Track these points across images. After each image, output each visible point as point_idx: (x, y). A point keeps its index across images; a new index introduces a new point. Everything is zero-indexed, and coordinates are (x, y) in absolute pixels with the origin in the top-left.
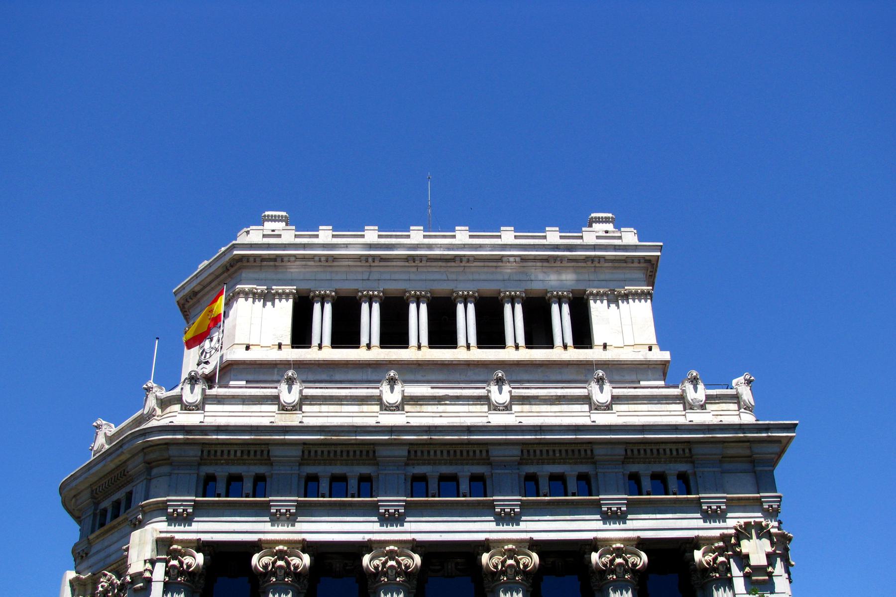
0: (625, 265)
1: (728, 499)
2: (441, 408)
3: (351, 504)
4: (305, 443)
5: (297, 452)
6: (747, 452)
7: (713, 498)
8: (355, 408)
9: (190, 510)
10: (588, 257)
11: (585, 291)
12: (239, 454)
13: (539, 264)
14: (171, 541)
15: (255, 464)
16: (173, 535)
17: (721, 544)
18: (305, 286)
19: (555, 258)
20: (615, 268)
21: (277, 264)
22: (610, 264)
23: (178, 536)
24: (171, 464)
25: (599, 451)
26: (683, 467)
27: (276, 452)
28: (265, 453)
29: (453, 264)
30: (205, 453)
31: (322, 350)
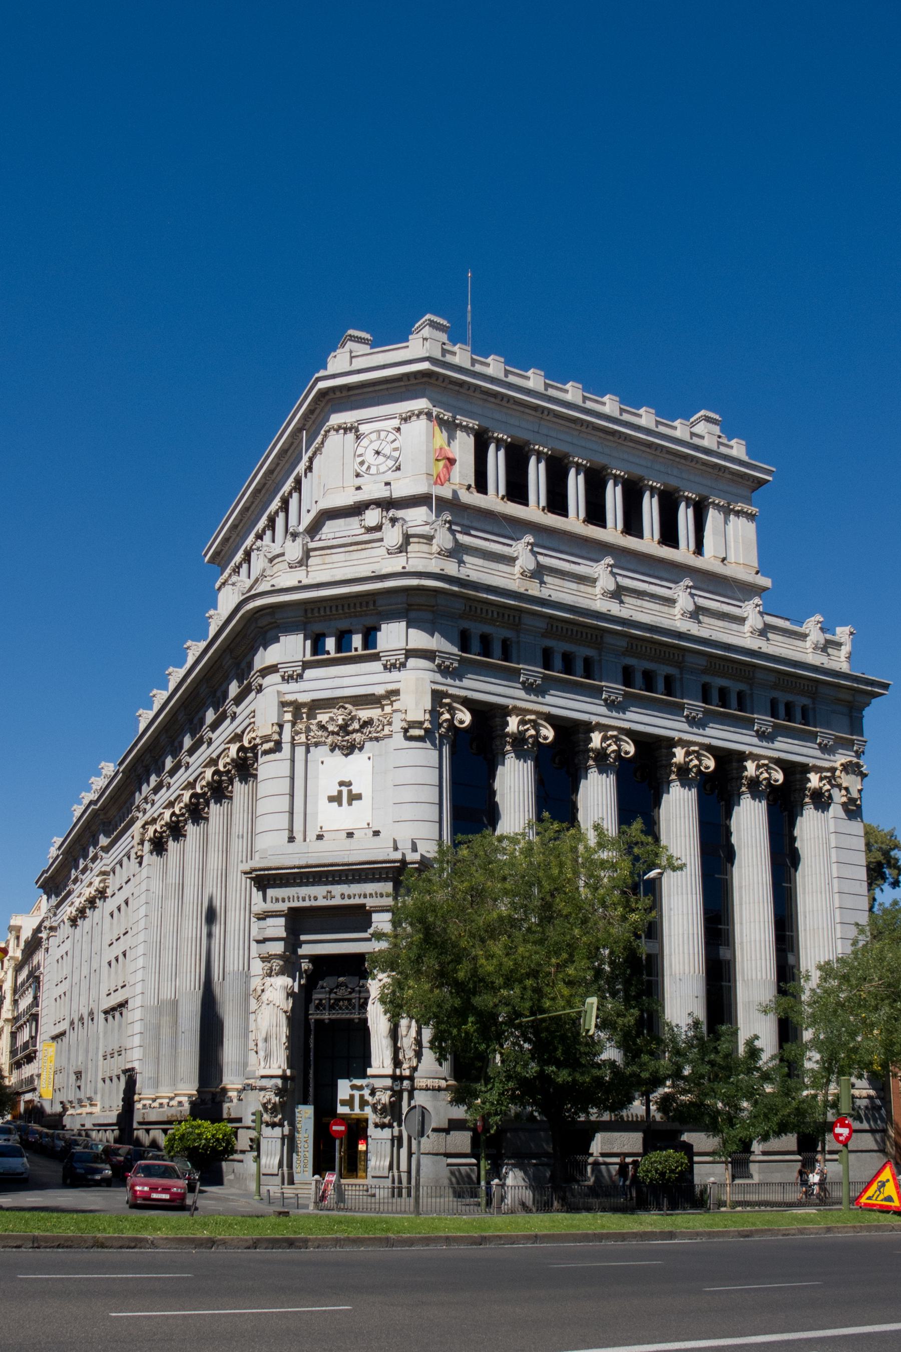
0: (740, 480)
1: (837, 737)
2: (639, 602)
3: (582, 684)
4: (551, 617)
5: (542, 625)
6: (849, 698)
7: (826, 735)
8: (574, 586)
9: (456, 665)
10: (716, 465)
11: (707, 498)
12: (495, 615)
13: (678, 460)
14: (446, 695)
15: (503, 627)
16: (448, 688)
17: (829, 774)
18: (487, 424)
19: (693, 458)
20: (733, 481)
21: (461, 390)
22: (730, 476)
23: (451, 691)
24: (433, 612)
25: (759, 675)
26: (806, 701)
27: (527, 620)
28: (517, 618)
29: (611, 438)
30: (468, 608)
31: (494, 500)
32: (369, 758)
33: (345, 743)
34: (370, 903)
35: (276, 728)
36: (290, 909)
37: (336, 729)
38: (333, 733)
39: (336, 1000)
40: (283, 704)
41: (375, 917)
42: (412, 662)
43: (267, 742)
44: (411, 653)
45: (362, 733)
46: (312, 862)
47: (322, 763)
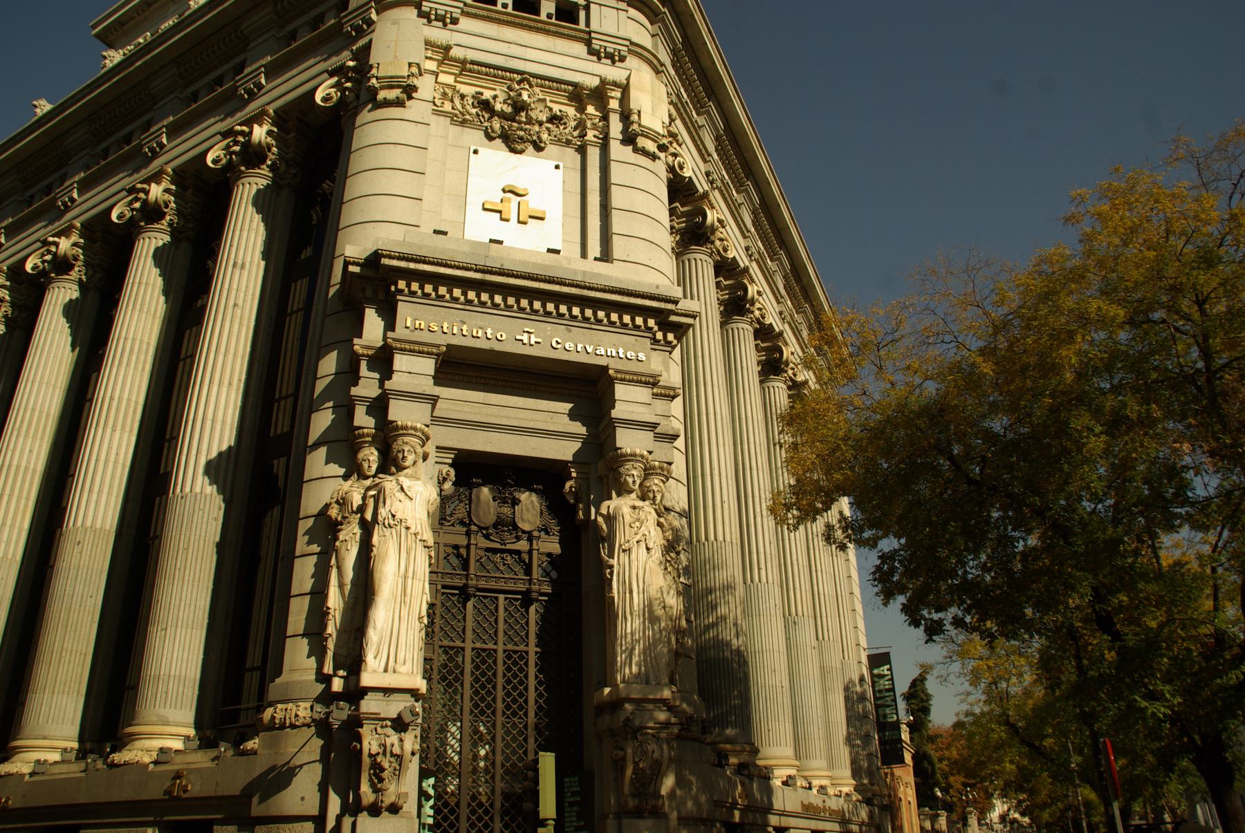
32: (557, 167)
33: (522, 133)
34: (613, 365)
35: (415, 70)
36: (448, 346)
37: (508, 109)
38: (502, 115)
39: (488, 550)
40: (428, 43)
41: (621, 391)
42: (632, 62)
43: (391, 87)
44: (636, 49)
45: (548, 129)
46: (508, 266)
47: (476, 152)
